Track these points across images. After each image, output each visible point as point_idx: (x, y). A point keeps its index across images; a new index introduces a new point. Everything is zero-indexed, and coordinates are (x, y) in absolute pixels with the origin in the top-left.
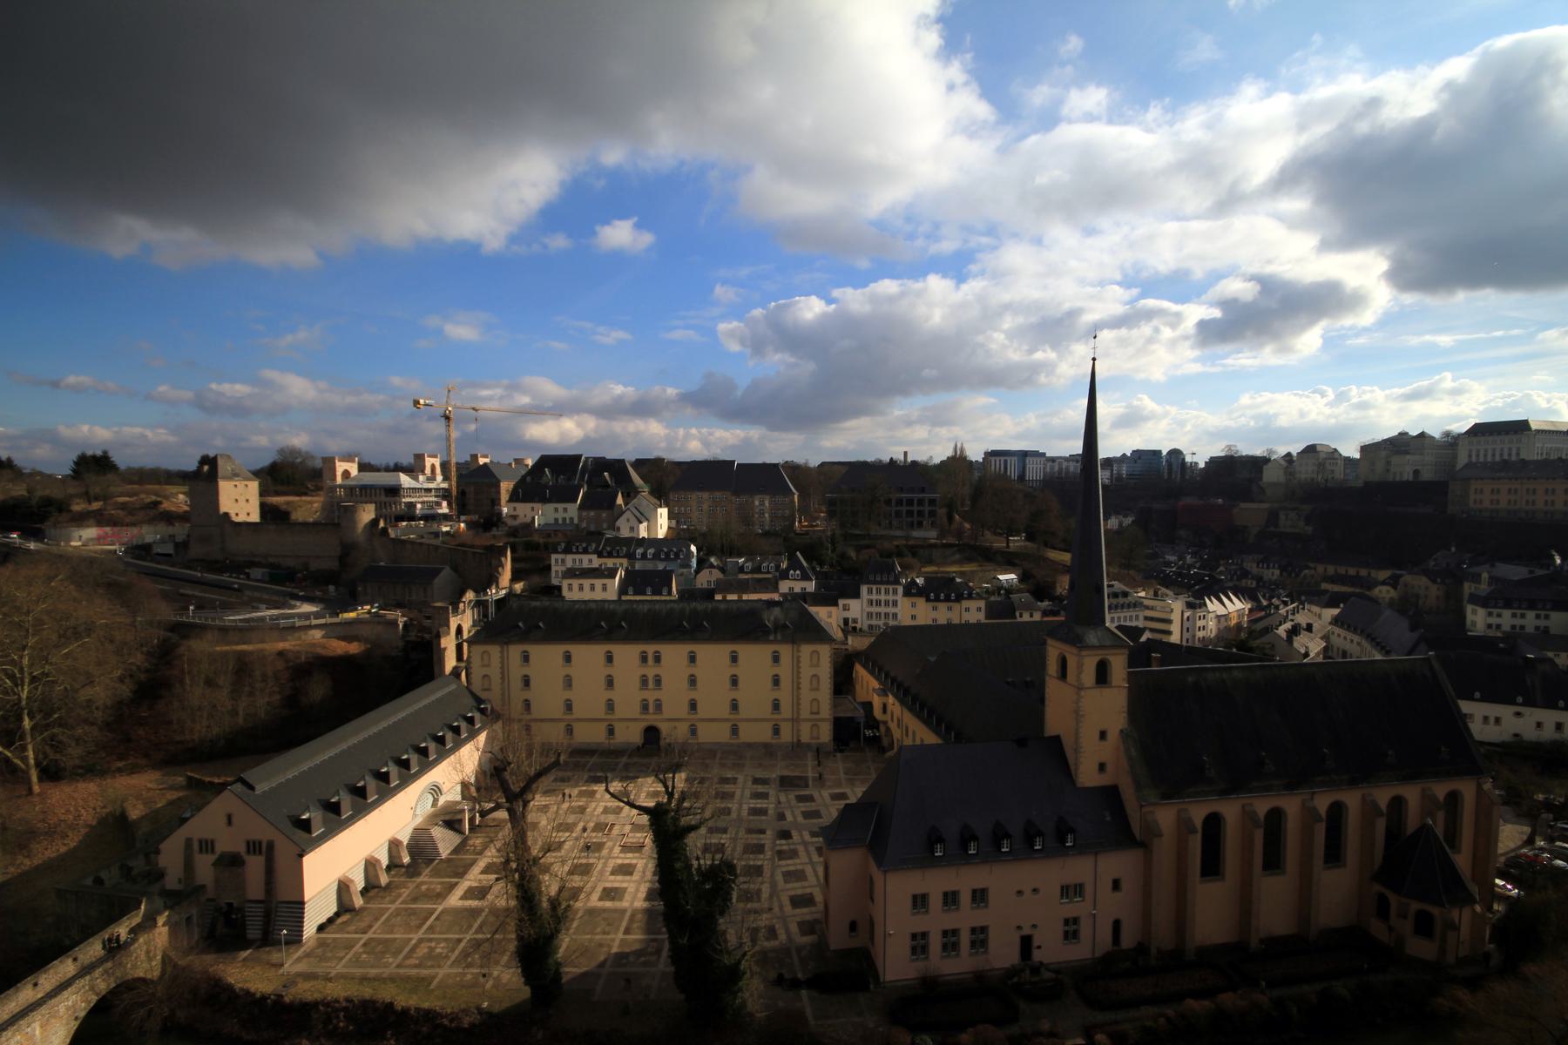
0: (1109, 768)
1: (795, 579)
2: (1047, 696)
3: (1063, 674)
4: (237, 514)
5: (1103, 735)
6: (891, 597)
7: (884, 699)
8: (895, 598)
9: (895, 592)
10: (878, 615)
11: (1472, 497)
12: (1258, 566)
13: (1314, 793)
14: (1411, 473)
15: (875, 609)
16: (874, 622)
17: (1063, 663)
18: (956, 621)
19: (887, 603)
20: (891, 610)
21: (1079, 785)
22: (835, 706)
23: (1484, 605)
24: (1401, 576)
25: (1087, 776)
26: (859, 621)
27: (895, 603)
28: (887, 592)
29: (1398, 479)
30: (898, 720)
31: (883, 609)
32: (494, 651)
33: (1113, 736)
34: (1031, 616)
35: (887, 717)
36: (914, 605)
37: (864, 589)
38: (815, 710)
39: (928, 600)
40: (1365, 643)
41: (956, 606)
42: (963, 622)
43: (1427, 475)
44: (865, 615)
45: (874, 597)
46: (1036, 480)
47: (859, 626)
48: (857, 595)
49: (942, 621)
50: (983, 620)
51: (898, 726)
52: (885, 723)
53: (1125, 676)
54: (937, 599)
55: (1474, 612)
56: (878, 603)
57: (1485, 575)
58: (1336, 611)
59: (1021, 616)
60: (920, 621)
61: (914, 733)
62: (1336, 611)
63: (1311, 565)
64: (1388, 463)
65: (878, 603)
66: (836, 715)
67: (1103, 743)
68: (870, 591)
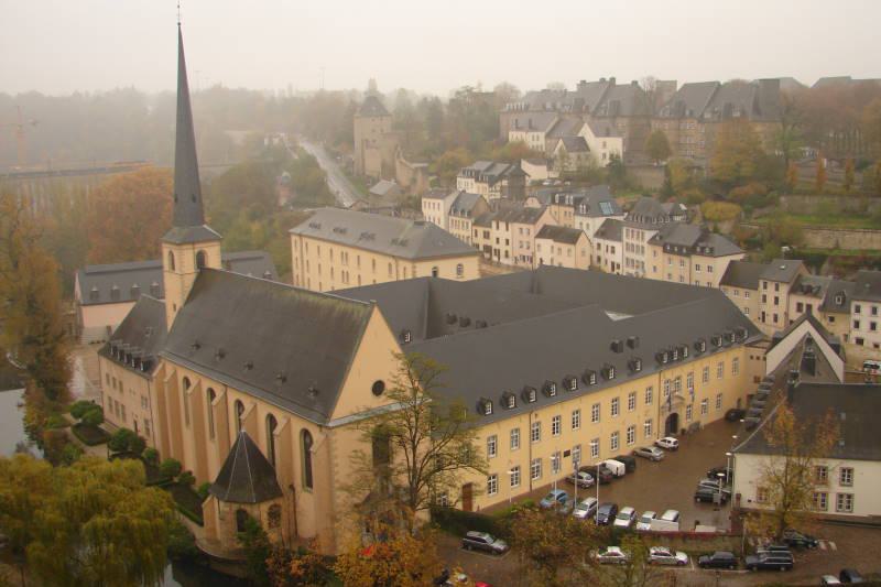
1: (582, 215)
4: (374, 141)
28: (638, 238)
32: (298, 238)
39: (665, 251)
41: (686, 260)
42: (693, 283)
45: (630, 241)
47: (620, 272)
48: (619, 239)
49: (675, 279)
54: (672, 252)
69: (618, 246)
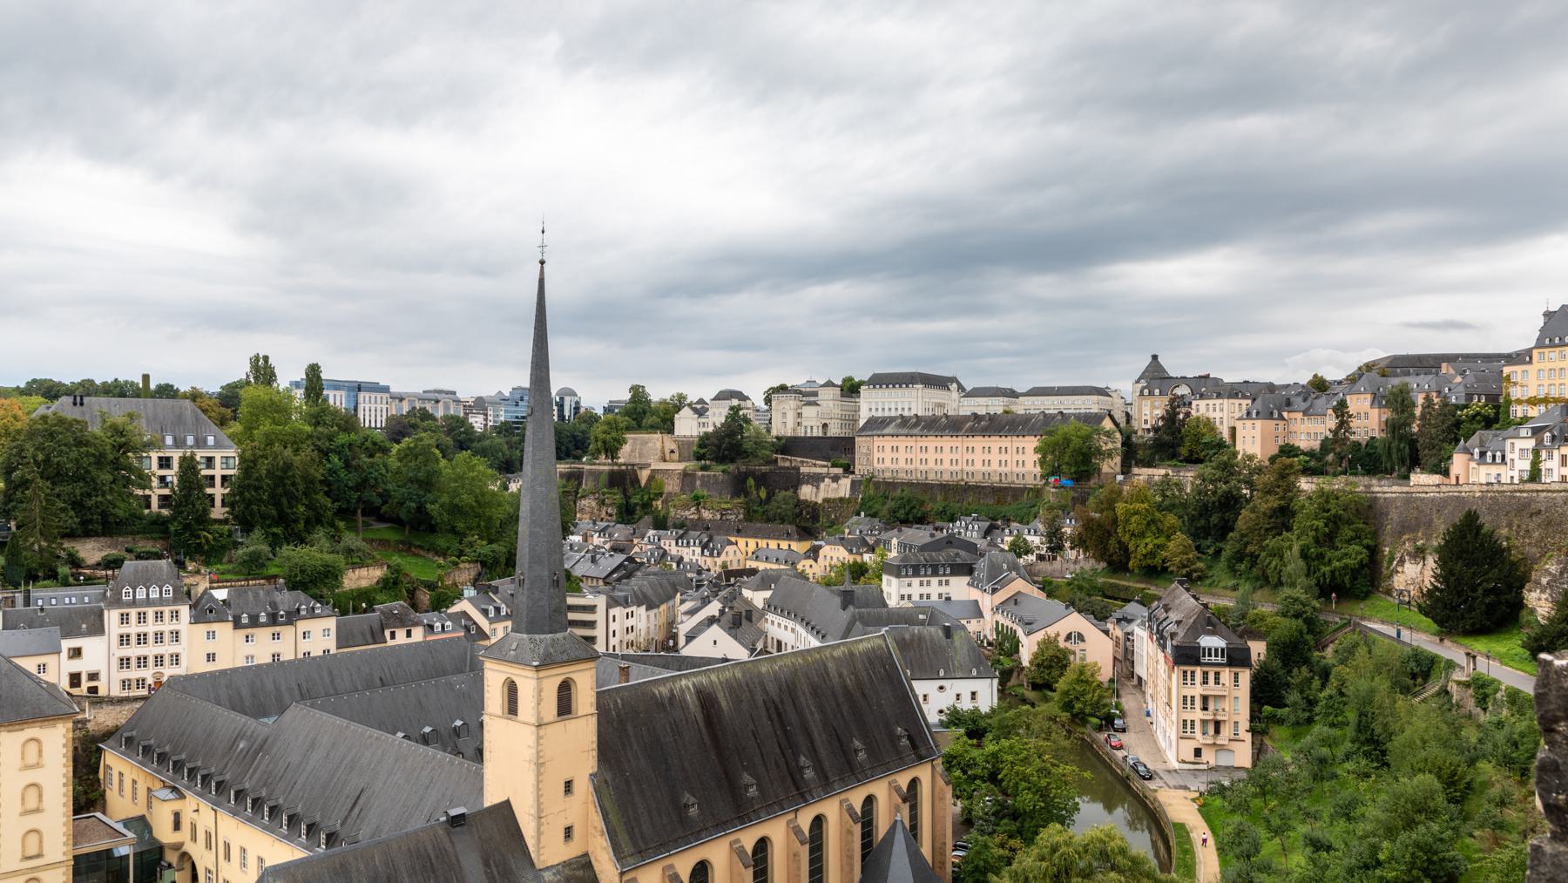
0: (576, 833)
2: (486, 744)
3: (512, 708)
5: (568, 786)
6: (166, 627)
7: (177, 805)
8: (174, 627)
9: (175, 615)
10: (142, 661)
11: (876, 455)
12: (677, 543)
13: (797, 810)
14: (821, 428)
15: (133, 651)
16: (134, 674)
17: (512, 690)
18: (287, 656)
19: (159, 637)
20: (166, 649)
21: (539, 866)
22: (77, 837)
23: (898, 576)
24: (820, 547)
25: (548, 851)
26: (103, 676)
27: (176, 636)
28: (159, 616)
29: (809, 435)
30: (208, 835)
31: (150, 650)
33: (583, 787)
34: (409, 634)
35: (183, 836)
36: (211, 635)
37: (112, 617)
38: (33, 851)
39: (237, 625)
40: (800, 629)
41: (287, 632)
43: (834, 431)
44: (115, 663)
45: (133, 629)
46: (376, 428)
48: (98, 629)
50: (333, 651)
51: (208, 846)
52: (177, 847)
53: (594, 700)
54: (254, 622)
55: (889, 584)
56: (142, 639)
57: (895, 541)
58: (768, 594)
59: (393, 636)
60: (221, 664)
61: (243, 850)
62: (768, 594)
63: (733, 539)
64: (800, 415)
65: (142, 639)
66: (87, 848)
67: (570, 798)
68: (124, 619)
69: (88, 644)
